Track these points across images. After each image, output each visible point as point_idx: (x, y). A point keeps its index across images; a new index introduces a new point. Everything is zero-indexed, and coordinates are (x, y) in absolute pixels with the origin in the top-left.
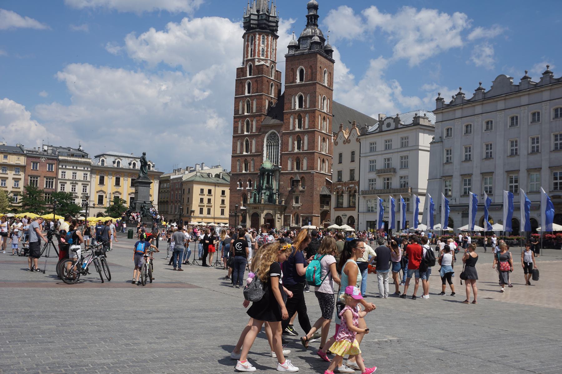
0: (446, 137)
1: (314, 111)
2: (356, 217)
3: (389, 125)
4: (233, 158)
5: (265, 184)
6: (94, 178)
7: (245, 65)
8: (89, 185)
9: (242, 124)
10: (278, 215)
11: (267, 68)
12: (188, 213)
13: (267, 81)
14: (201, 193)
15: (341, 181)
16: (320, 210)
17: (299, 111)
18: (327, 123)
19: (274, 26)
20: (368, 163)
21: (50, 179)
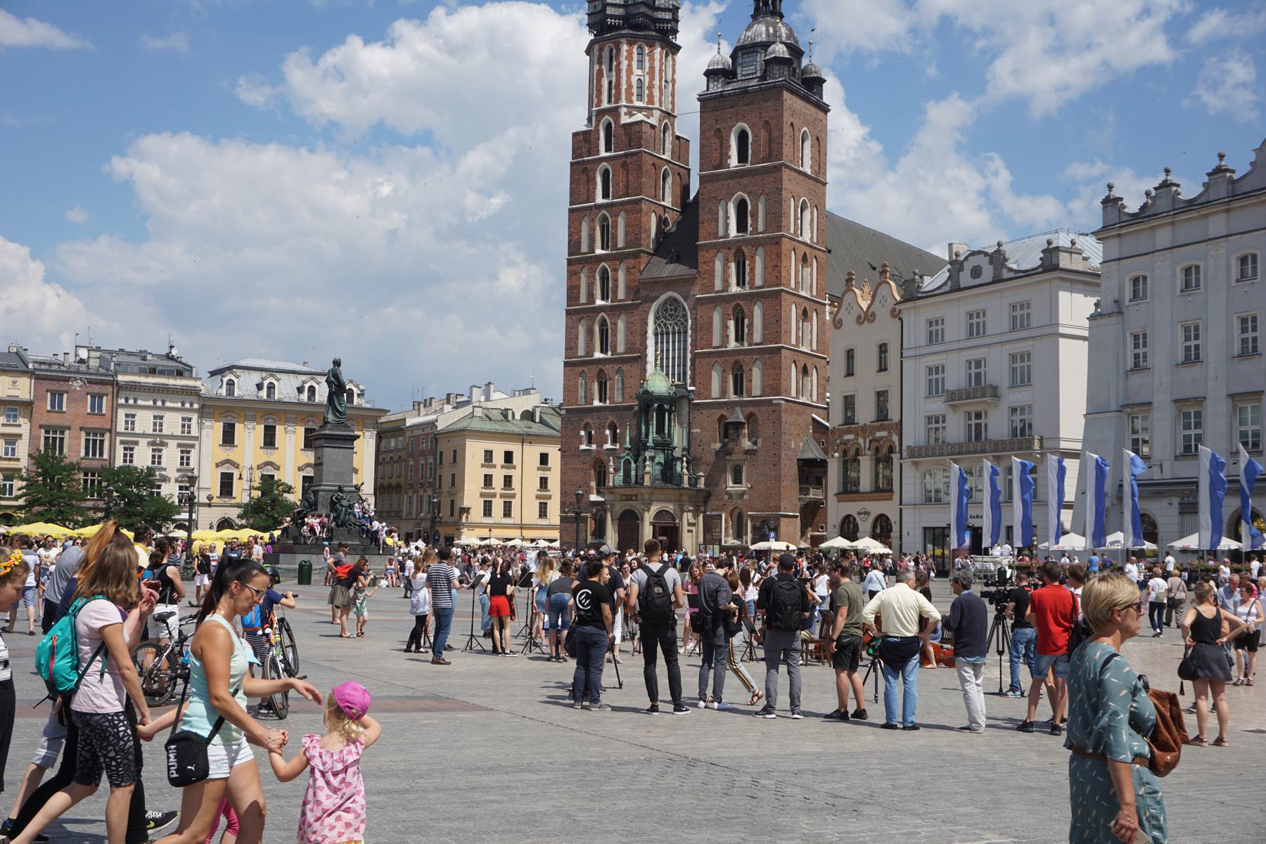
0: (1131, 300)
1: (777, 241)
2: (894, 518)
3: (976, 272)
4: (568, 368)
5: (653, 435)
6: (208, 430)
8: (197, 447)
9: (589, 277)
10: (688, 517)
11: (651, 131)
12: (452, 514)
13: (654, 164)
14: (485, 460)
15: (854, 423)
16: (800, 499)
17: (739, 241)
18: (812, 271)
19: (668, 21)
20: (923, 372)
21: (95, 435)
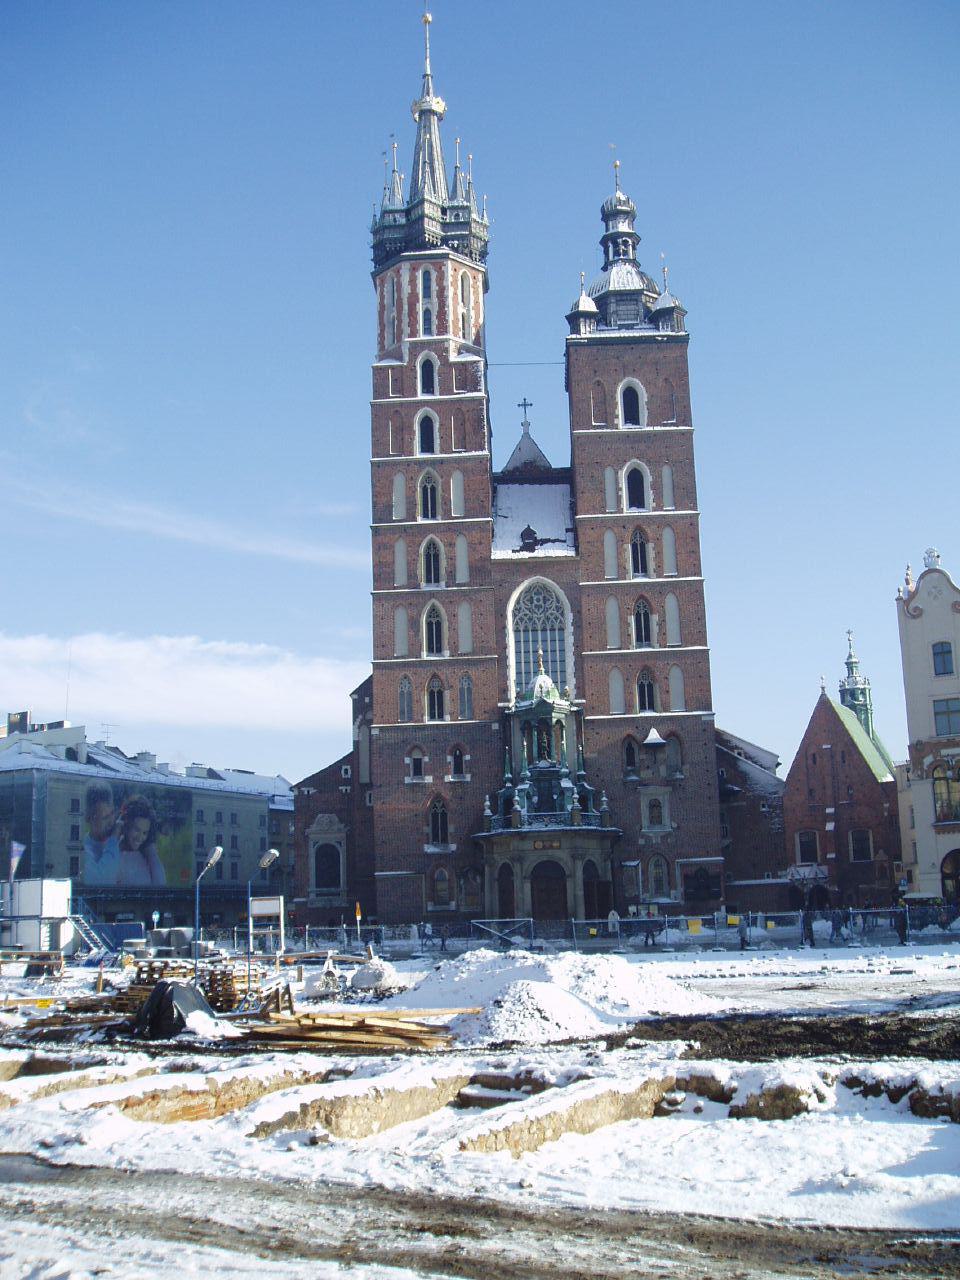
7: (406, 358)
9: (408, 553)
